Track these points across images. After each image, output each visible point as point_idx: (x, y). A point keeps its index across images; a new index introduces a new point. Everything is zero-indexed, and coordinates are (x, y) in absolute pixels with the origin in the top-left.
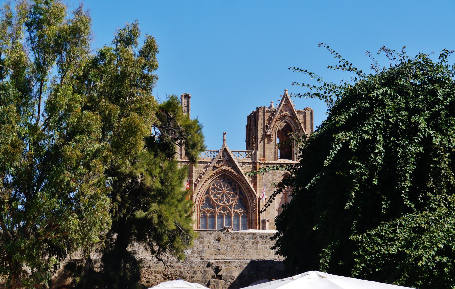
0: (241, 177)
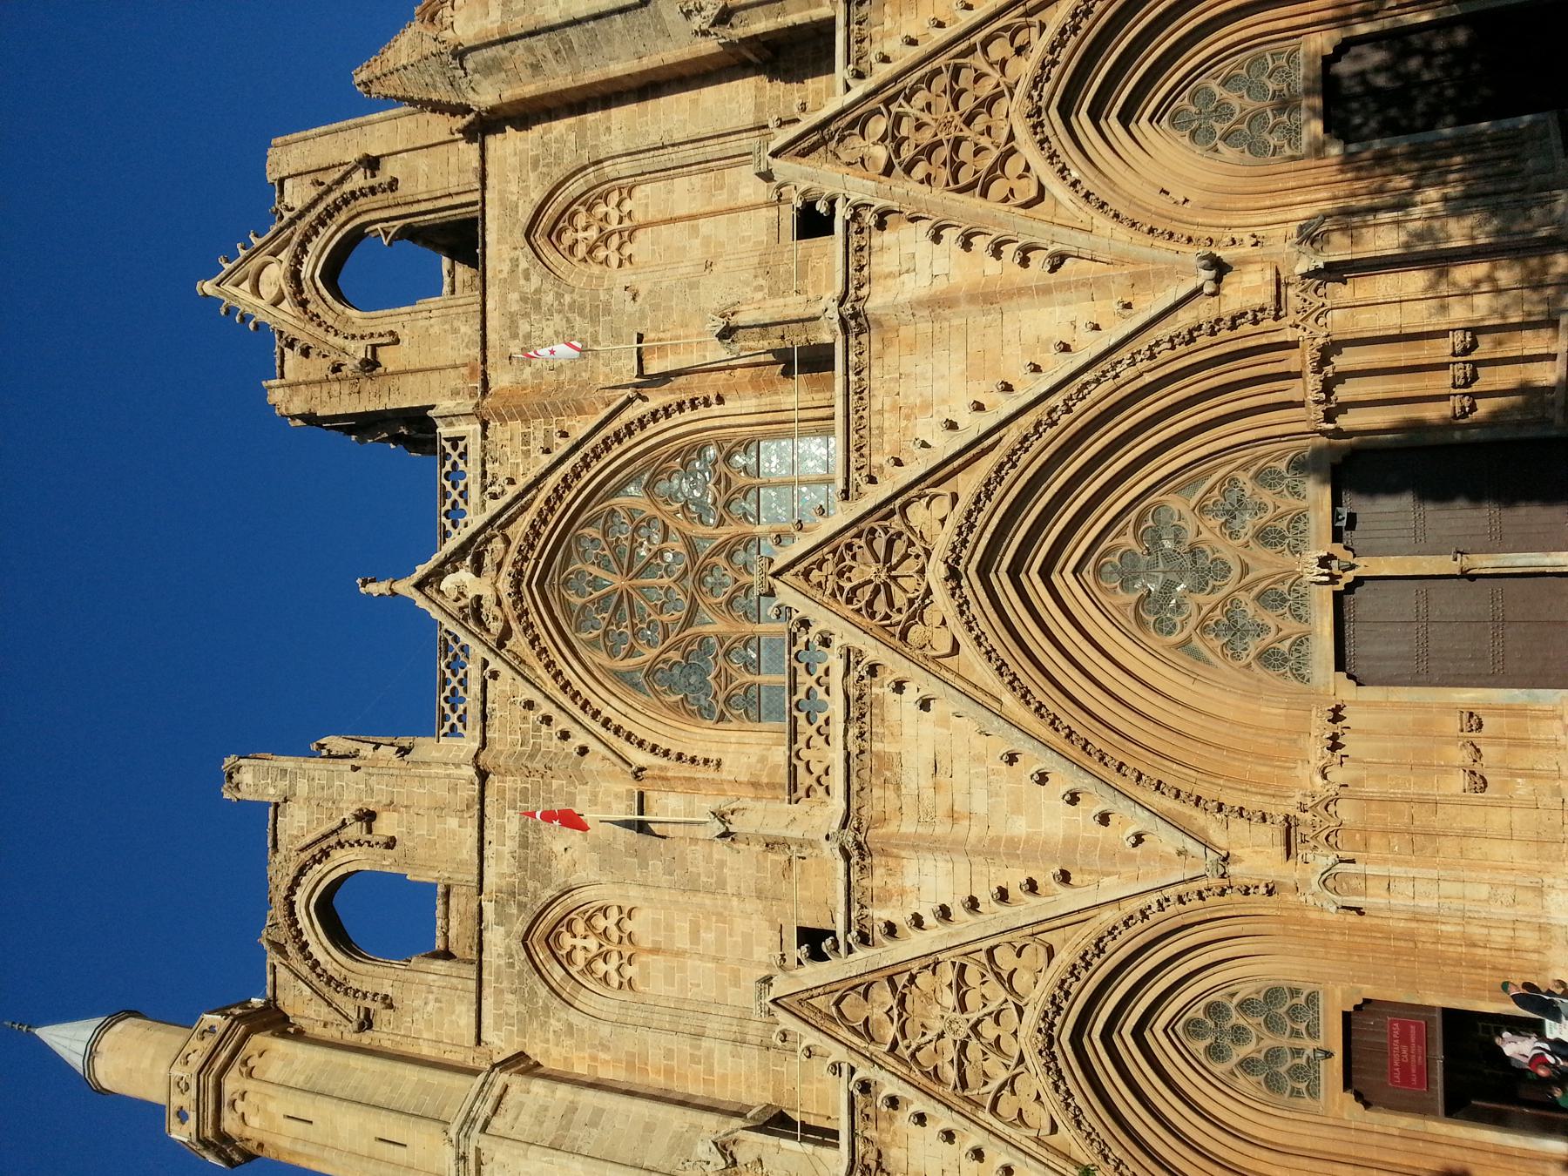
0: (542, 496)
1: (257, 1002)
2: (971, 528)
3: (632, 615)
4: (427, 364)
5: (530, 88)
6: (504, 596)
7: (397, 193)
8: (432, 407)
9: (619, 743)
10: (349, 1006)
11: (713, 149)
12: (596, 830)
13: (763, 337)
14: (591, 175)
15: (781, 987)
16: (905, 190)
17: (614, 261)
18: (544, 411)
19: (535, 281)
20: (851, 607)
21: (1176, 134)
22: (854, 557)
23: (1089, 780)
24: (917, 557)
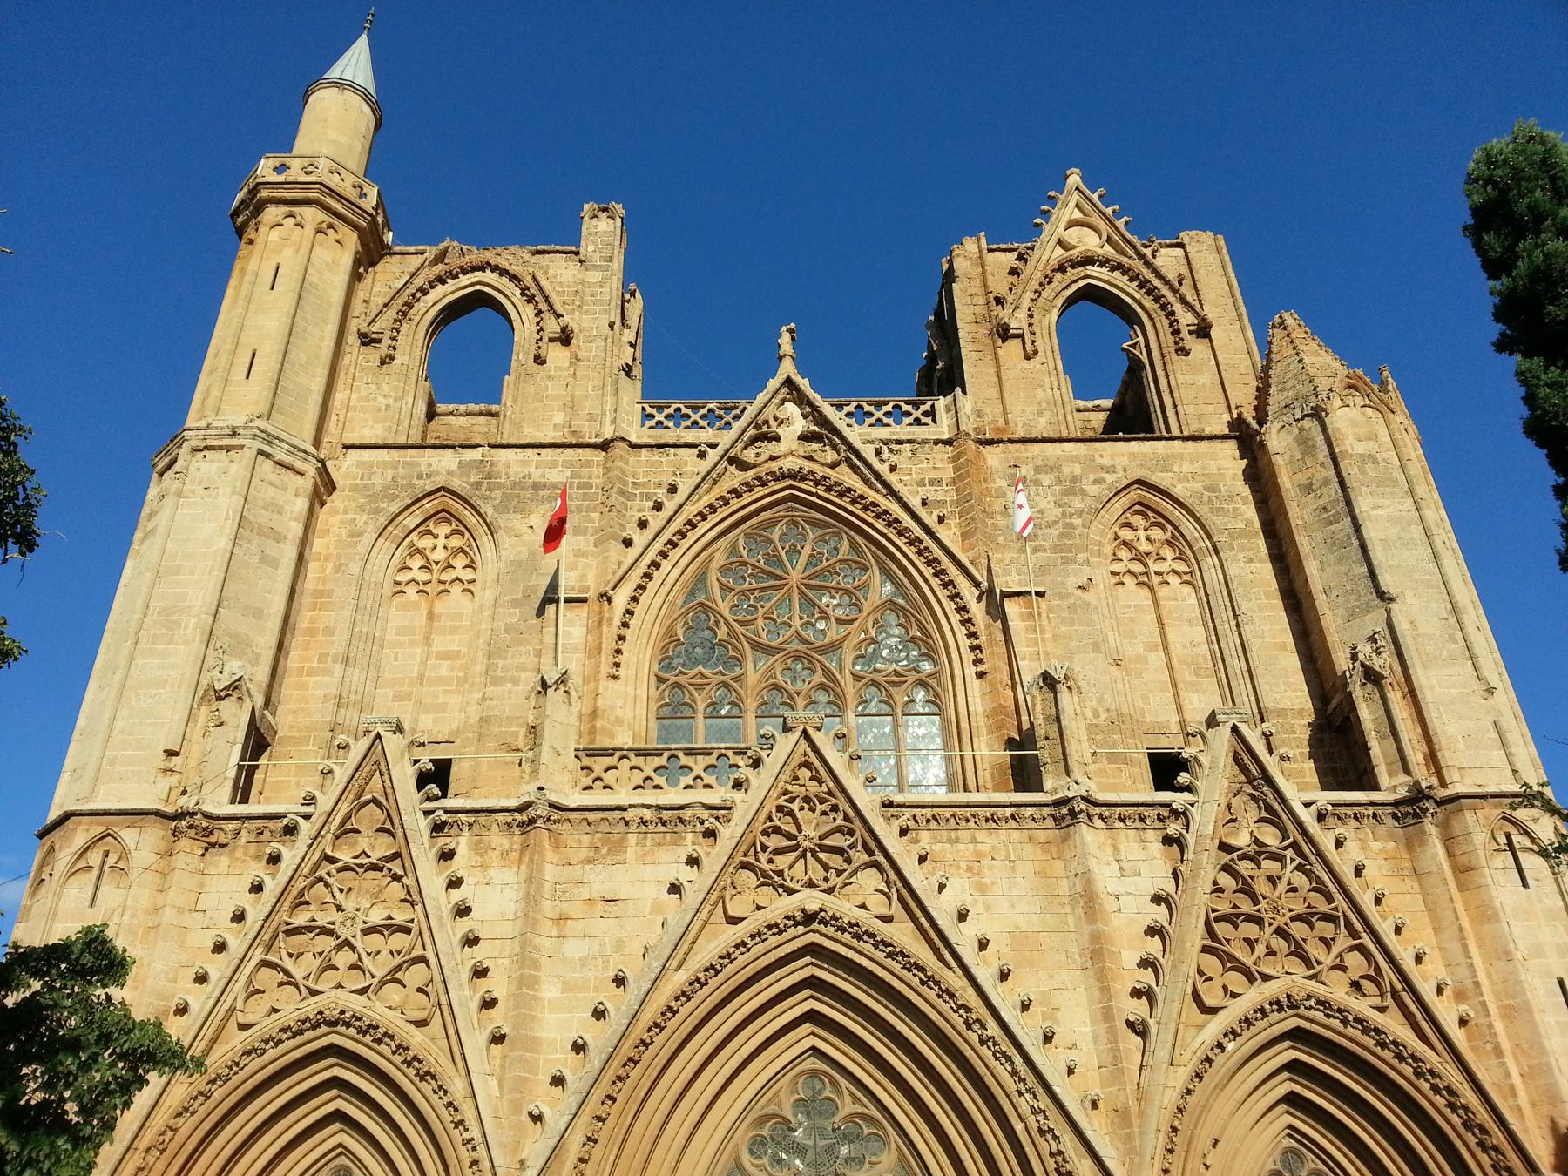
0: (880, 499)
1: (389, 237)
2: (857, 937)
3: (763, 589)
4: (1006, 386)
5: (1286, 482)
6: (779, 463)
7: (1174, 356)
8: (964, 392)
9: (635, 578)
10: (384, 323)
11: (1236, 666)
12: (551, 559)
13: (1046, 719)
14: (1202, 544)
15: (392, 742)
16: (1206, 866)
17: (1117, 567)
18: (964, 499)
19: (1093, 490)
20: (774, 811)
21: (1277, 1154)
22: (824, 813)
23: (597, 1064)
24: (826, 880)
